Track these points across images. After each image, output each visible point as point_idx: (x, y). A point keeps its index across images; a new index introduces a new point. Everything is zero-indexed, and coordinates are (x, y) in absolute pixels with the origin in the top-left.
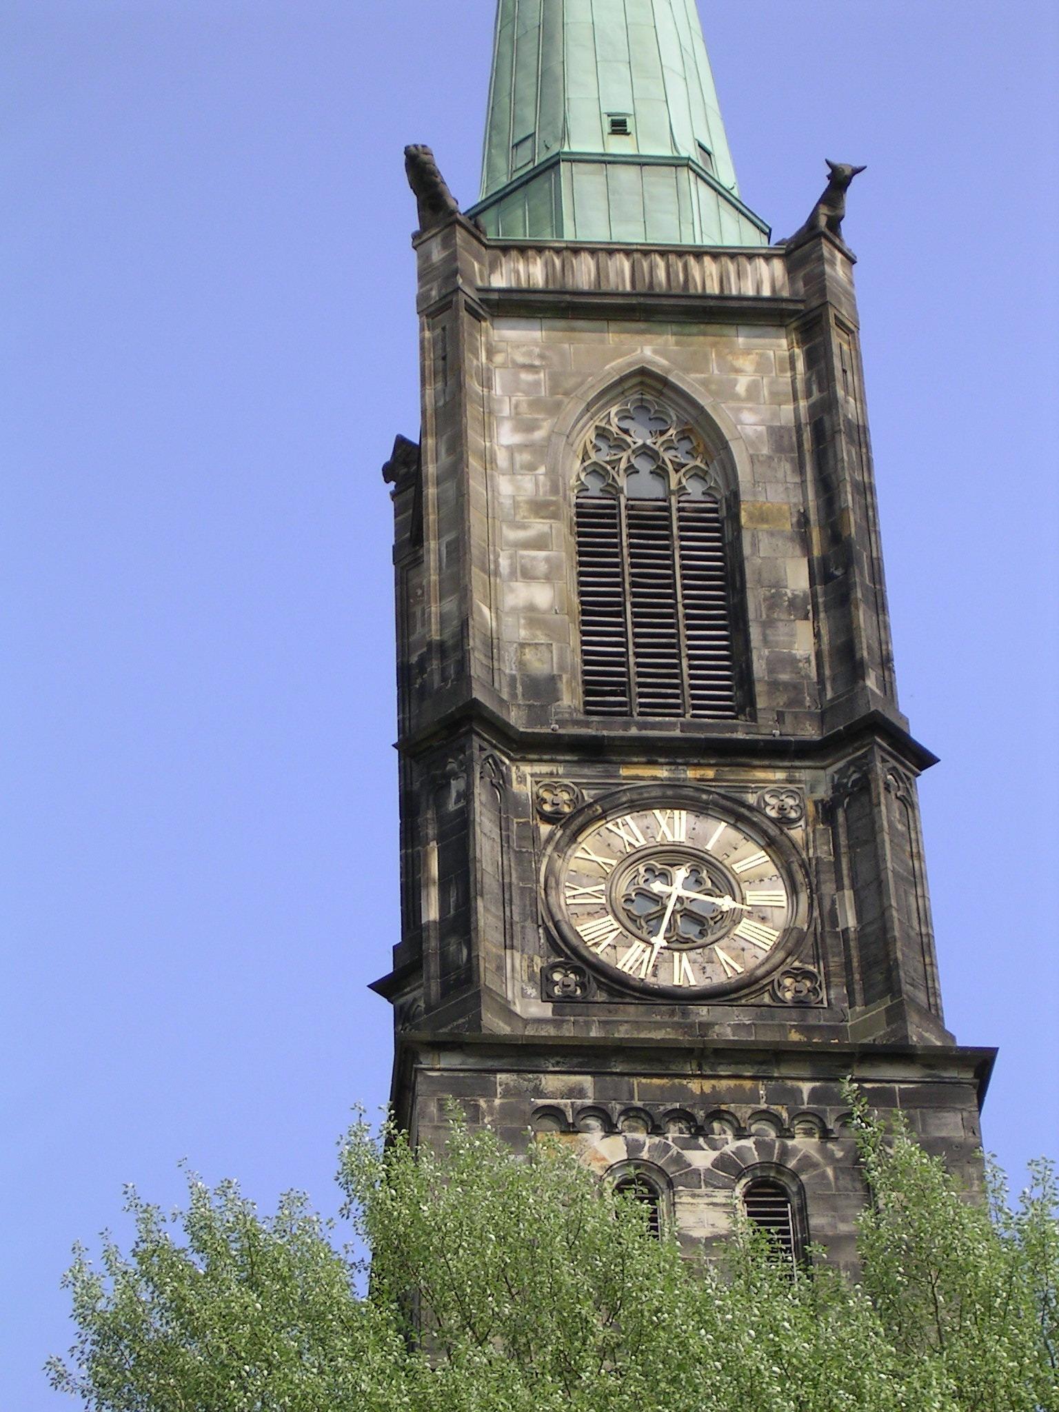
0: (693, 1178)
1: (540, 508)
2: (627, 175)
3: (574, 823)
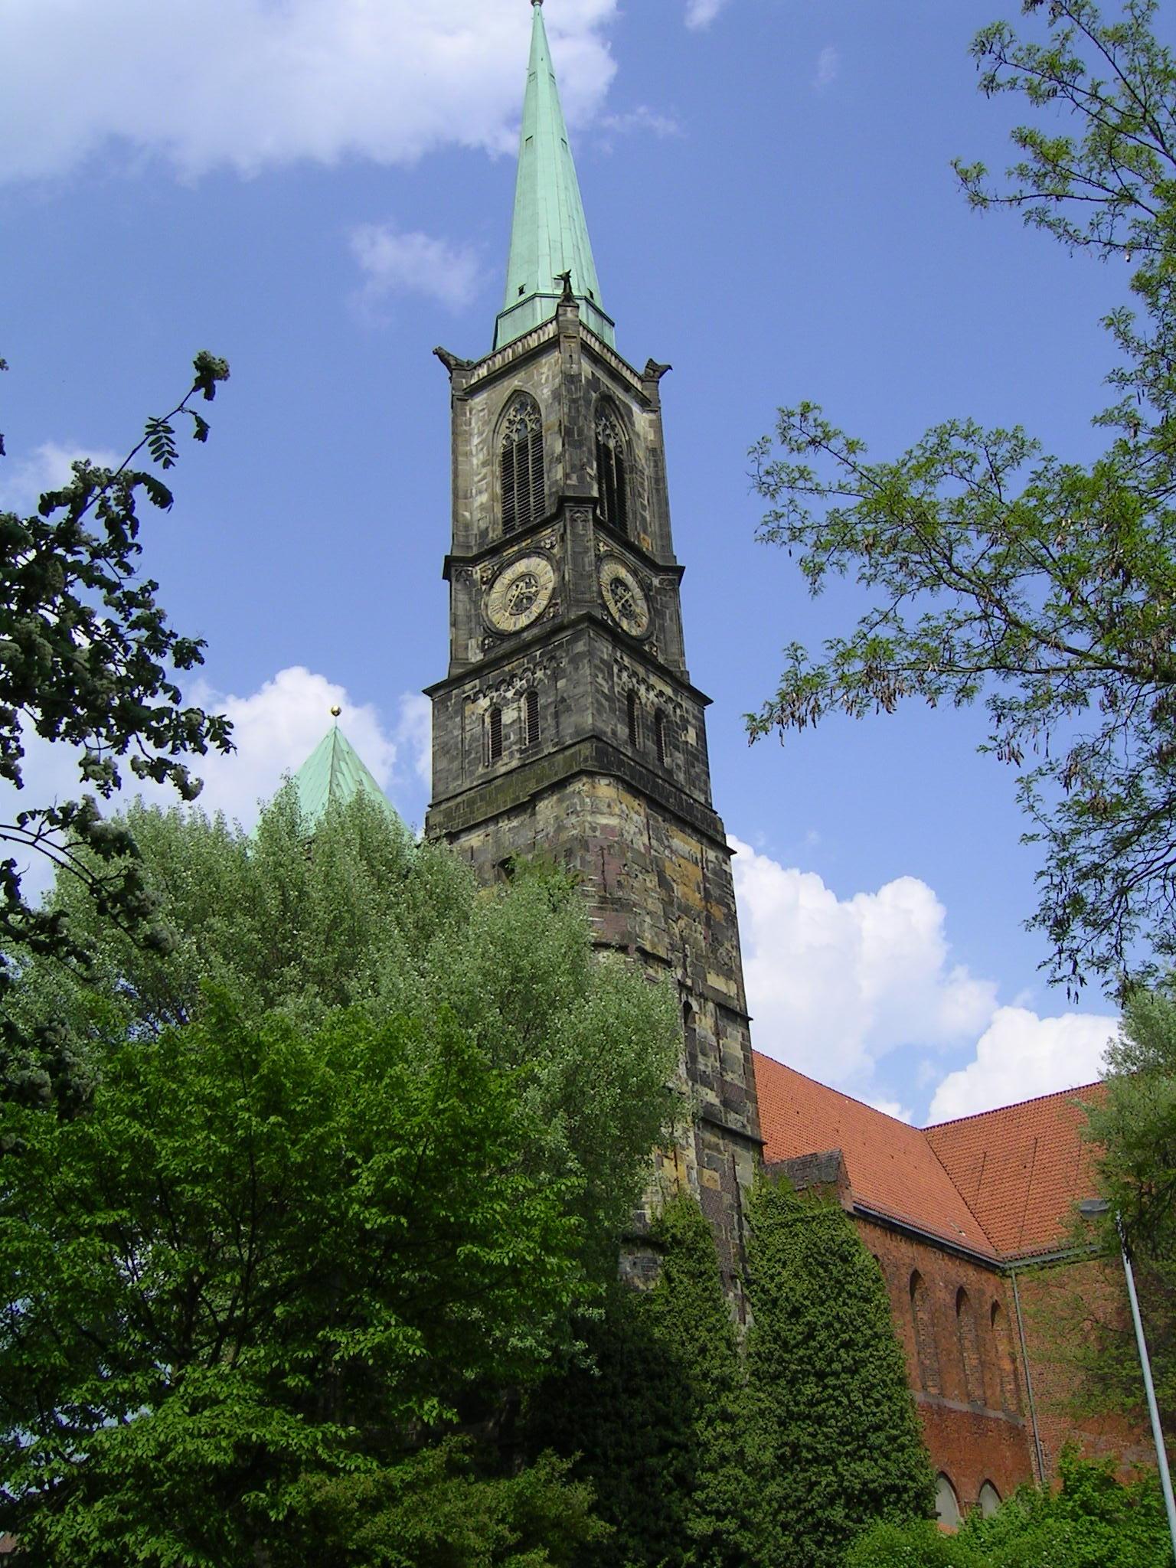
1: (484, 464)
3: (491, 583)
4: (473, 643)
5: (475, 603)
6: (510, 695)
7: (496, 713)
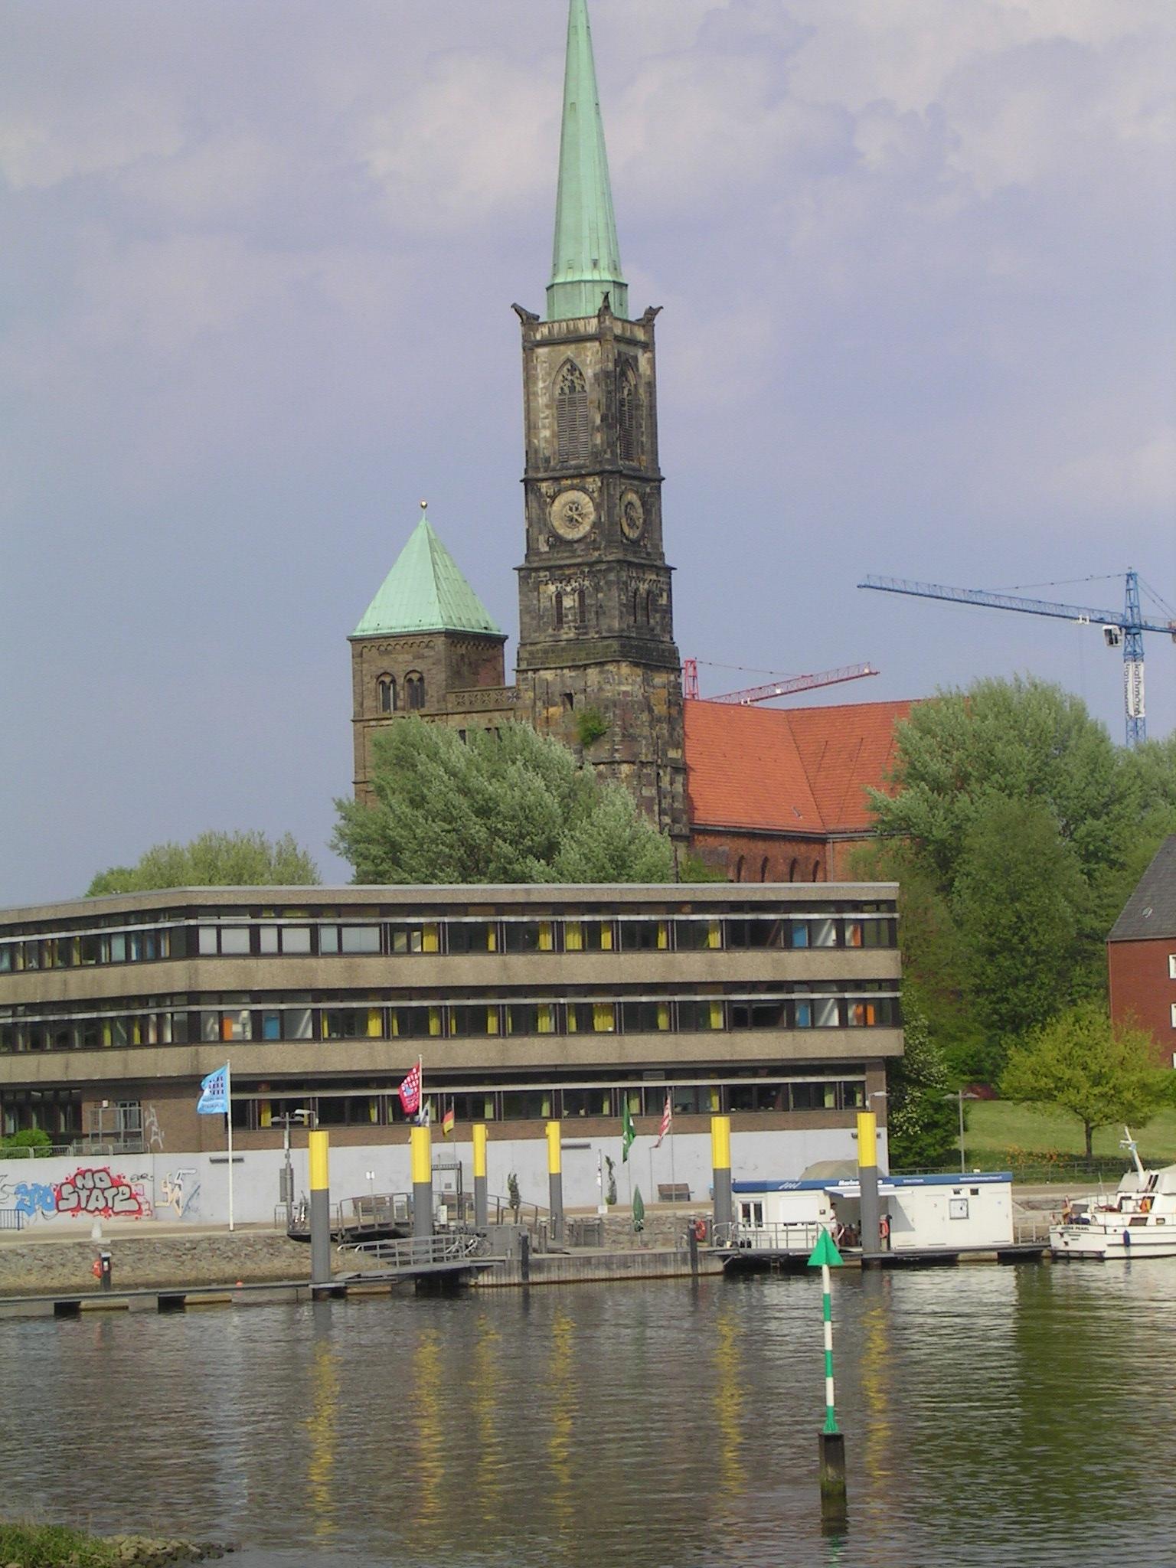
0: (567, 594)
1: (547, 406)
2: (569, 287)
3: (553, 498)
4: (541, 538)
5: (543, 510)
6: (569, 589)
7: (559, 596)
